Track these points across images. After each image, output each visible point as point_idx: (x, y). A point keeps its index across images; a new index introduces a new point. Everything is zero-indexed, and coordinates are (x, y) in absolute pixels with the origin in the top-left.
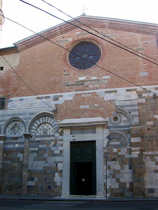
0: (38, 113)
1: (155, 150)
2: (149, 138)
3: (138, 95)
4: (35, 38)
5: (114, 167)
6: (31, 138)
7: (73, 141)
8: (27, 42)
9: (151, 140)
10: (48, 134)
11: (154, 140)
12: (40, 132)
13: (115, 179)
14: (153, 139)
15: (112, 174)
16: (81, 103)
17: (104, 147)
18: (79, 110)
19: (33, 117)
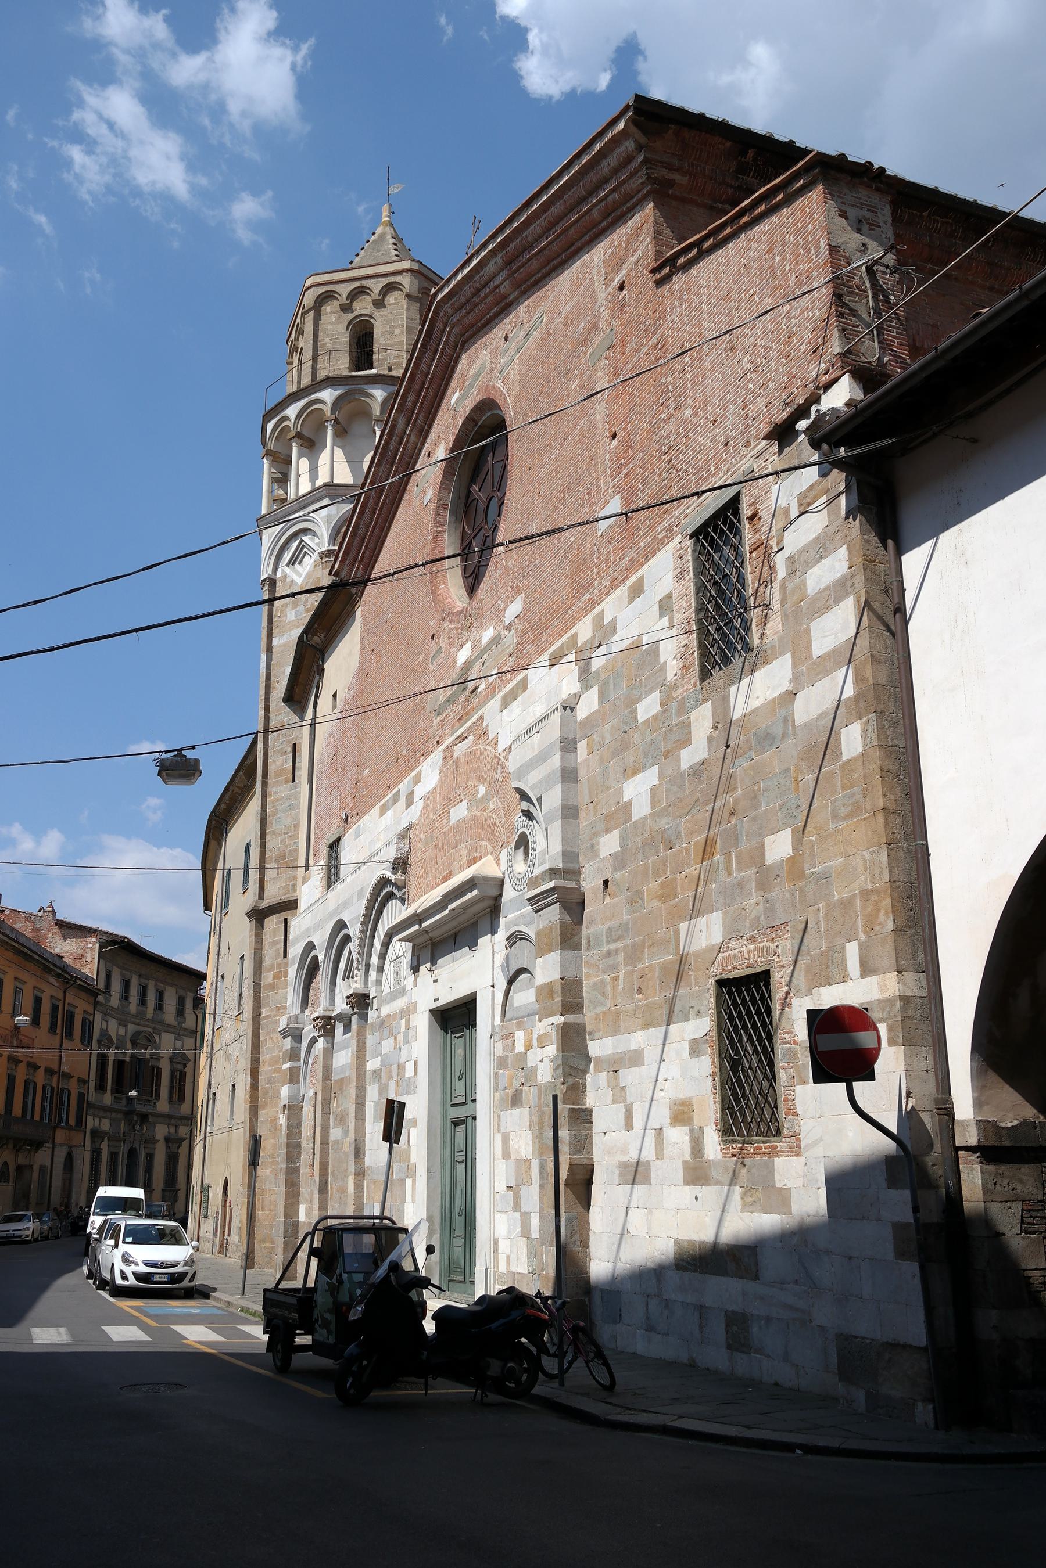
0: (370, 889)
1: (622, 1032)
2: (605, 948)
3: (579, 668)
4: (368, 512)
5: (517, 1146)
6: (372, 1010)
7: (434, 1005)
8: (356, 541)
9: (610, 961)
10: (402, 984)
11: (621, 957)
12: (388, 977)
13: (518, 1215)
14: (617, 951)
15: (512, 1184)
16: (451, 796)
17: (493, 1026)
18: (450, 830)
19: (363, 910)
